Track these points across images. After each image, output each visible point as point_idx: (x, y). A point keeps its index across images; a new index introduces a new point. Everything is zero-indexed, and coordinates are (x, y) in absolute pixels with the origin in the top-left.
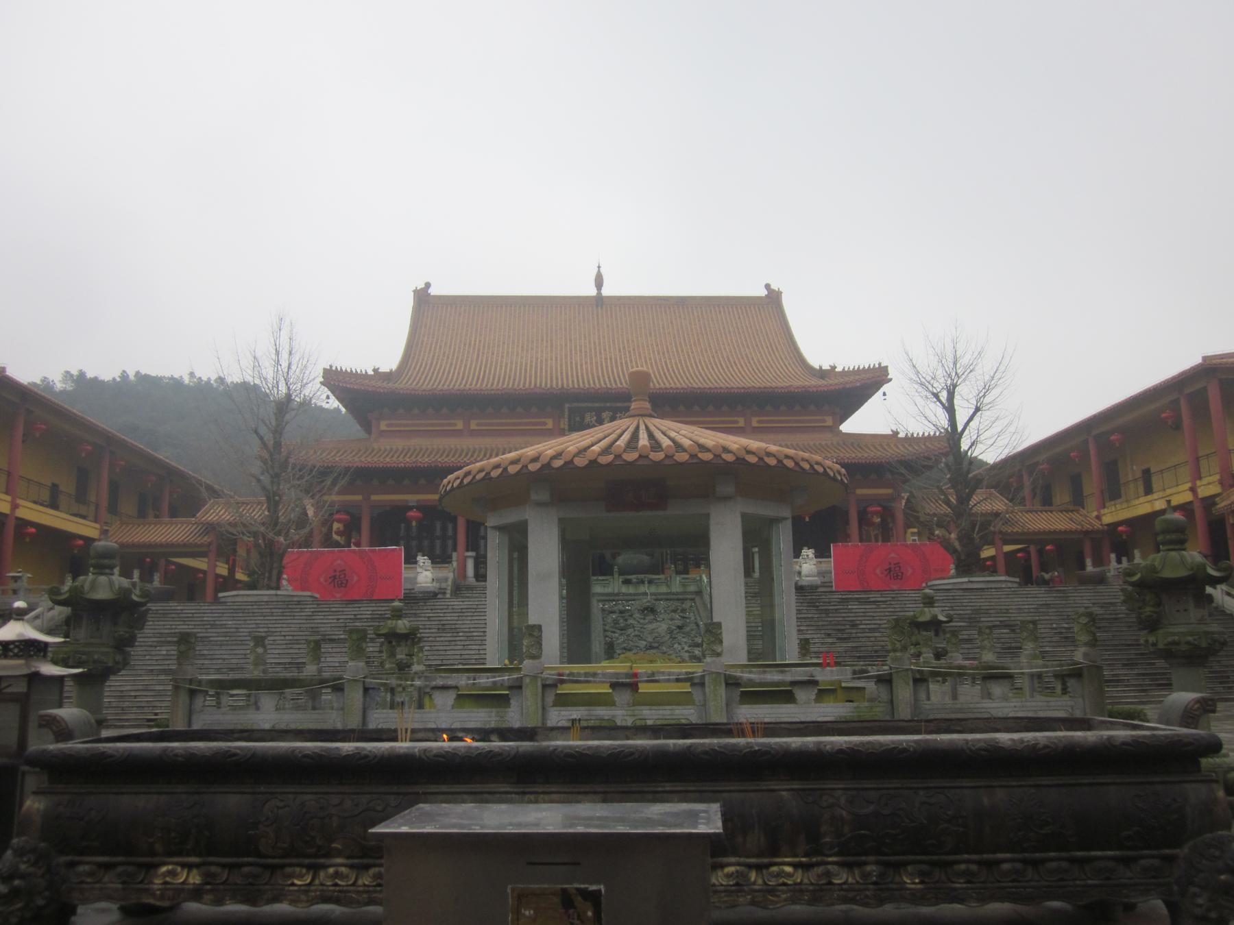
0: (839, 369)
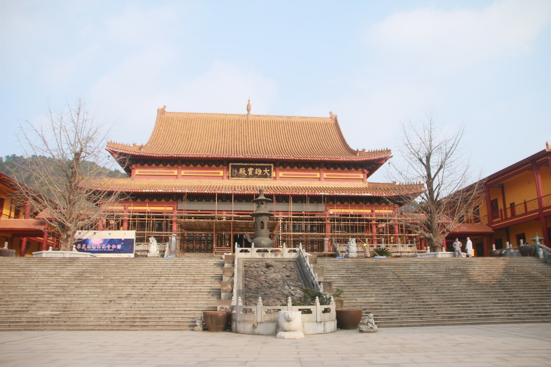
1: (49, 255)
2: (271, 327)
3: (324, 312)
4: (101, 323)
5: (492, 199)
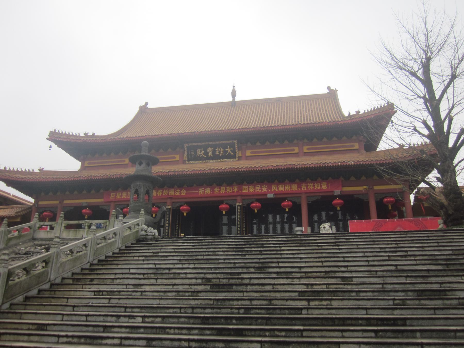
0: (362, 112)
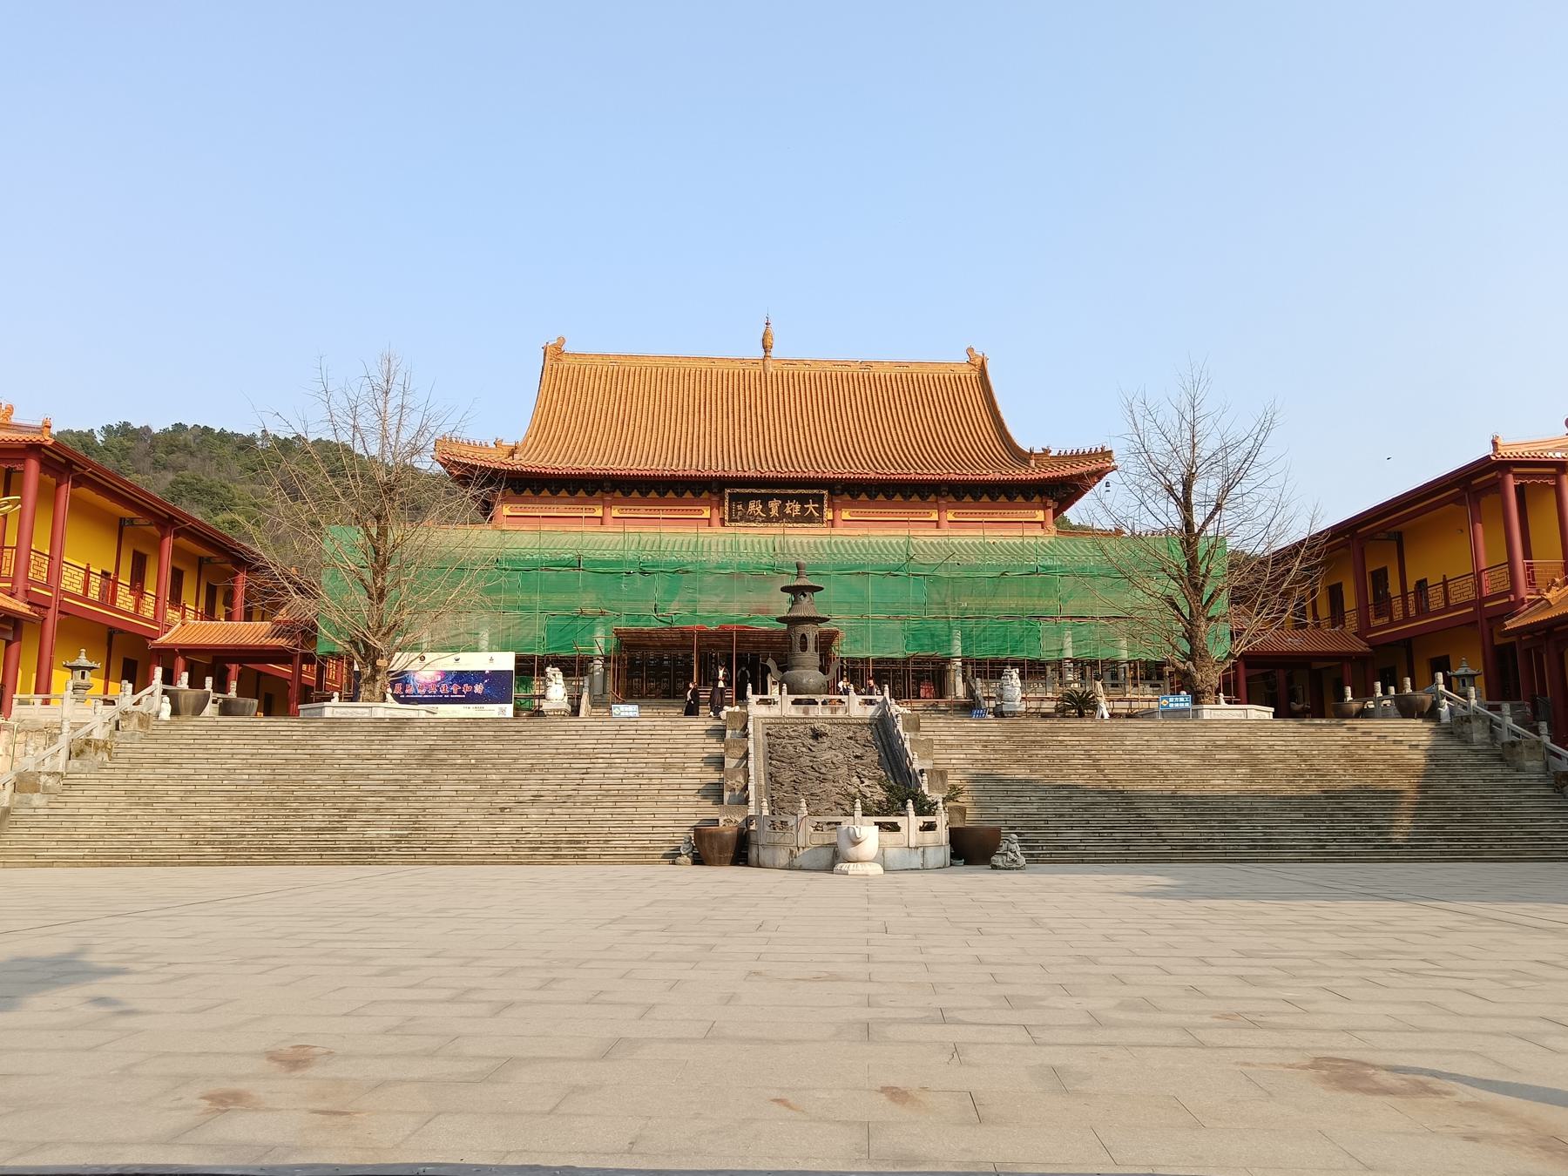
0: (1054, 453)
1: (338, 713)
2: (826, 855)
3: (921, 829)
4: (493, 851)
5: (1371, 568)
